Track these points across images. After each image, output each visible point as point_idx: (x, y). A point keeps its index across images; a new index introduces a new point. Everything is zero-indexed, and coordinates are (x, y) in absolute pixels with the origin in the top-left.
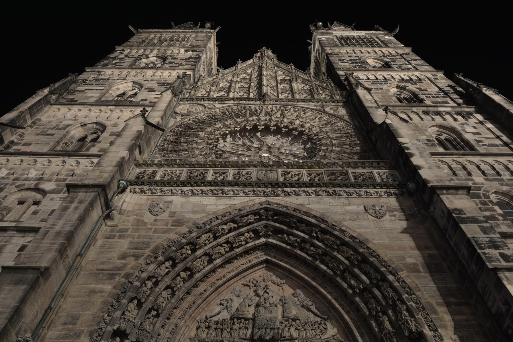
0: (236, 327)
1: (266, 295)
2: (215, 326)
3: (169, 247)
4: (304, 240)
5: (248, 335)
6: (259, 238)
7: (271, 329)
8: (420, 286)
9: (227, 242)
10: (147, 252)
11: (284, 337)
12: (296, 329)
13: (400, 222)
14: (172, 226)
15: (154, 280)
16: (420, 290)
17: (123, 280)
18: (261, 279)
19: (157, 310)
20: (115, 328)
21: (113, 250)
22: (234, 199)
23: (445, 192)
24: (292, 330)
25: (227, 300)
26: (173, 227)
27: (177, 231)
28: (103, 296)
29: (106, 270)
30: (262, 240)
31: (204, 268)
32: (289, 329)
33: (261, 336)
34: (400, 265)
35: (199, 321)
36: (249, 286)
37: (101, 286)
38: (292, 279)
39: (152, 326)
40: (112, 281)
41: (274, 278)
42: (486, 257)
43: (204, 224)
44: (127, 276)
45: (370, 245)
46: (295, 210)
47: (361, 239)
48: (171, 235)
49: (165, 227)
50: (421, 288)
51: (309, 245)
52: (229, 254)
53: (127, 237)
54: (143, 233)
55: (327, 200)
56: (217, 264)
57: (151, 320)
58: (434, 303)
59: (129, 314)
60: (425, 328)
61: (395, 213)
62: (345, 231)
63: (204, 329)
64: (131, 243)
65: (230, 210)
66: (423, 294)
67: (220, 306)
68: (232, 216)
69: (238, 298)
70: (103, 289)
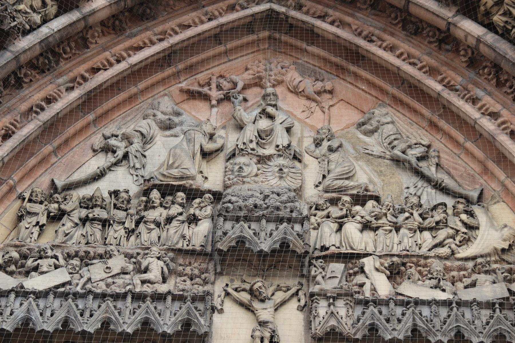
1: (264, 124)
2: (84, 213)
7: (280, 220)
11: (324, 248)
12: (366, 226)
18: (247, 76)
24: (352, 228)
25: (127, 139)
31: (45, 21)
32: (341, 226)
33: (241, 241)
35: (27, 195)
36: (206, 98)
38: (356, 75)
41: (293, 76)
56: (93, 13)
63: (43, 220)
69: (168, 133)
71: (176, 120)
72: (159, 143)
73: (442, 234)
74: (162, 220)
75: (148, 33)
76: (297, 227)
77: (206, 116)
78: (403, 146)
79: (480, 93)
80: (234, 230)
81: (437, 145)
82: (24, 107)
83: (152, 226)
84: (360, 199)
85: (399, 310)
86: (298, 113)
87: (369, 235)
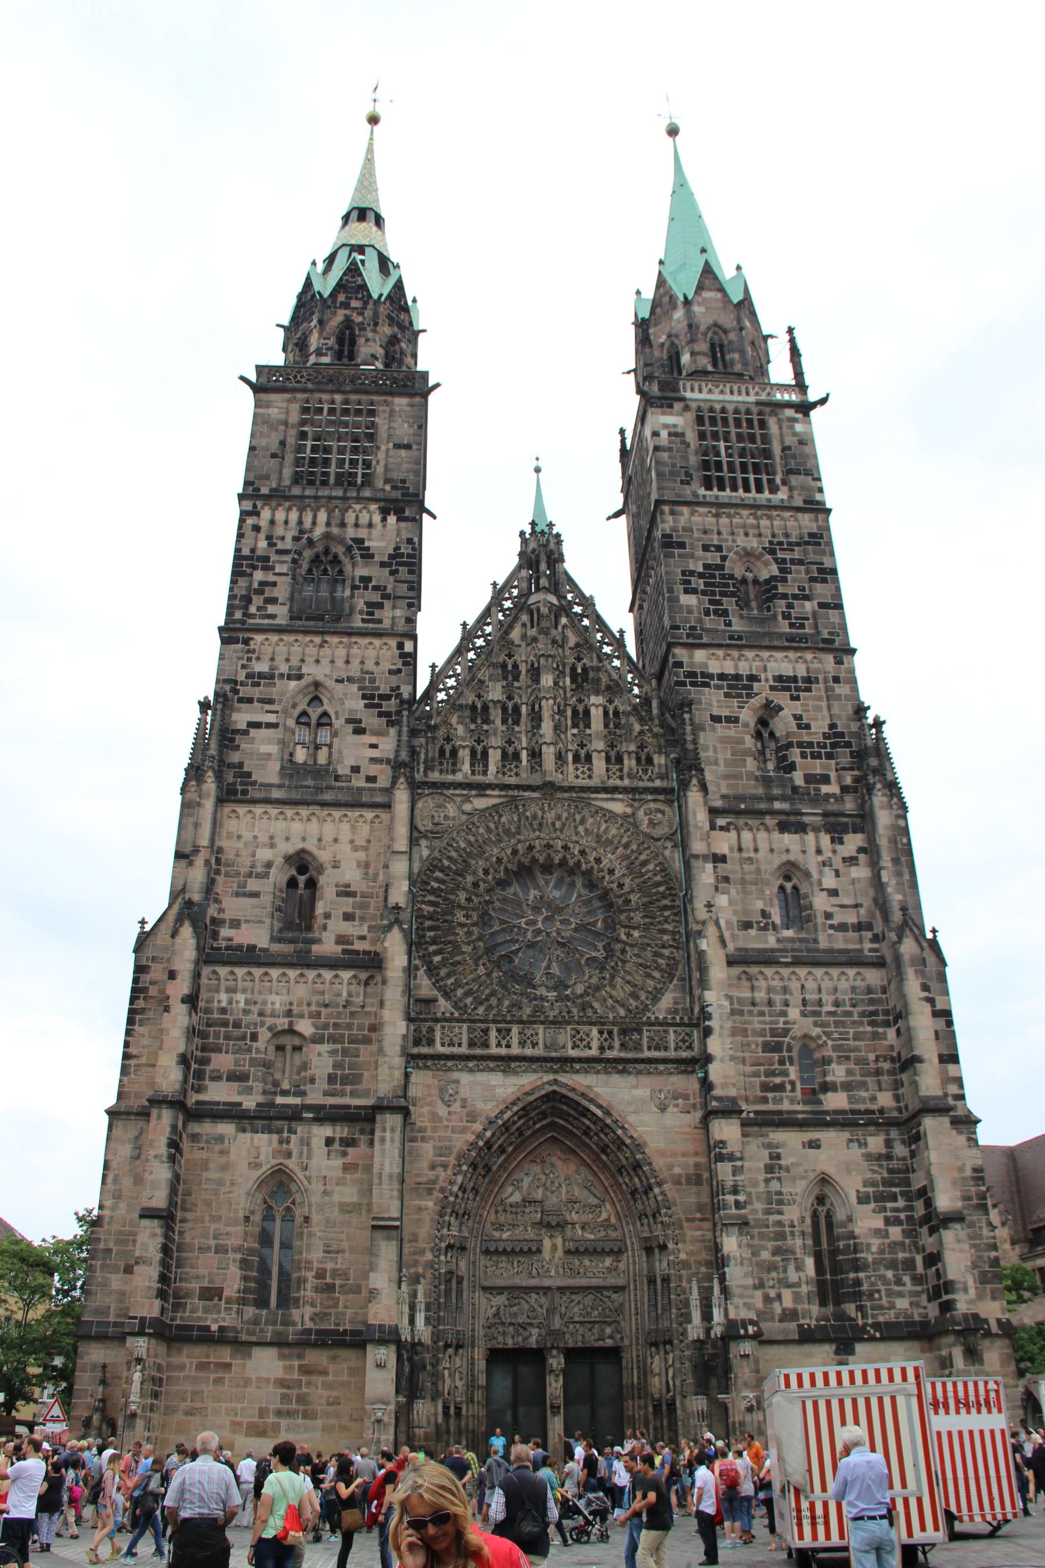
0: (527, 1210)
4: (588, 1128)
5: (538, 1220)
6: (545, 1117)
9: (518, 1129)
10: (452, 1160)
17: (441, 1196)
37: (423, 1203)
41: (559, 1153)
44: (442, 1190)
46: (583, 1095)
47: (640, 1141)
54: (442, 1134)
55: (616, 1078)
64: (435, 1147)
65: (519, 1095)
68: (521, 1105)
77: (536, 1168)
80: (546, 1219)
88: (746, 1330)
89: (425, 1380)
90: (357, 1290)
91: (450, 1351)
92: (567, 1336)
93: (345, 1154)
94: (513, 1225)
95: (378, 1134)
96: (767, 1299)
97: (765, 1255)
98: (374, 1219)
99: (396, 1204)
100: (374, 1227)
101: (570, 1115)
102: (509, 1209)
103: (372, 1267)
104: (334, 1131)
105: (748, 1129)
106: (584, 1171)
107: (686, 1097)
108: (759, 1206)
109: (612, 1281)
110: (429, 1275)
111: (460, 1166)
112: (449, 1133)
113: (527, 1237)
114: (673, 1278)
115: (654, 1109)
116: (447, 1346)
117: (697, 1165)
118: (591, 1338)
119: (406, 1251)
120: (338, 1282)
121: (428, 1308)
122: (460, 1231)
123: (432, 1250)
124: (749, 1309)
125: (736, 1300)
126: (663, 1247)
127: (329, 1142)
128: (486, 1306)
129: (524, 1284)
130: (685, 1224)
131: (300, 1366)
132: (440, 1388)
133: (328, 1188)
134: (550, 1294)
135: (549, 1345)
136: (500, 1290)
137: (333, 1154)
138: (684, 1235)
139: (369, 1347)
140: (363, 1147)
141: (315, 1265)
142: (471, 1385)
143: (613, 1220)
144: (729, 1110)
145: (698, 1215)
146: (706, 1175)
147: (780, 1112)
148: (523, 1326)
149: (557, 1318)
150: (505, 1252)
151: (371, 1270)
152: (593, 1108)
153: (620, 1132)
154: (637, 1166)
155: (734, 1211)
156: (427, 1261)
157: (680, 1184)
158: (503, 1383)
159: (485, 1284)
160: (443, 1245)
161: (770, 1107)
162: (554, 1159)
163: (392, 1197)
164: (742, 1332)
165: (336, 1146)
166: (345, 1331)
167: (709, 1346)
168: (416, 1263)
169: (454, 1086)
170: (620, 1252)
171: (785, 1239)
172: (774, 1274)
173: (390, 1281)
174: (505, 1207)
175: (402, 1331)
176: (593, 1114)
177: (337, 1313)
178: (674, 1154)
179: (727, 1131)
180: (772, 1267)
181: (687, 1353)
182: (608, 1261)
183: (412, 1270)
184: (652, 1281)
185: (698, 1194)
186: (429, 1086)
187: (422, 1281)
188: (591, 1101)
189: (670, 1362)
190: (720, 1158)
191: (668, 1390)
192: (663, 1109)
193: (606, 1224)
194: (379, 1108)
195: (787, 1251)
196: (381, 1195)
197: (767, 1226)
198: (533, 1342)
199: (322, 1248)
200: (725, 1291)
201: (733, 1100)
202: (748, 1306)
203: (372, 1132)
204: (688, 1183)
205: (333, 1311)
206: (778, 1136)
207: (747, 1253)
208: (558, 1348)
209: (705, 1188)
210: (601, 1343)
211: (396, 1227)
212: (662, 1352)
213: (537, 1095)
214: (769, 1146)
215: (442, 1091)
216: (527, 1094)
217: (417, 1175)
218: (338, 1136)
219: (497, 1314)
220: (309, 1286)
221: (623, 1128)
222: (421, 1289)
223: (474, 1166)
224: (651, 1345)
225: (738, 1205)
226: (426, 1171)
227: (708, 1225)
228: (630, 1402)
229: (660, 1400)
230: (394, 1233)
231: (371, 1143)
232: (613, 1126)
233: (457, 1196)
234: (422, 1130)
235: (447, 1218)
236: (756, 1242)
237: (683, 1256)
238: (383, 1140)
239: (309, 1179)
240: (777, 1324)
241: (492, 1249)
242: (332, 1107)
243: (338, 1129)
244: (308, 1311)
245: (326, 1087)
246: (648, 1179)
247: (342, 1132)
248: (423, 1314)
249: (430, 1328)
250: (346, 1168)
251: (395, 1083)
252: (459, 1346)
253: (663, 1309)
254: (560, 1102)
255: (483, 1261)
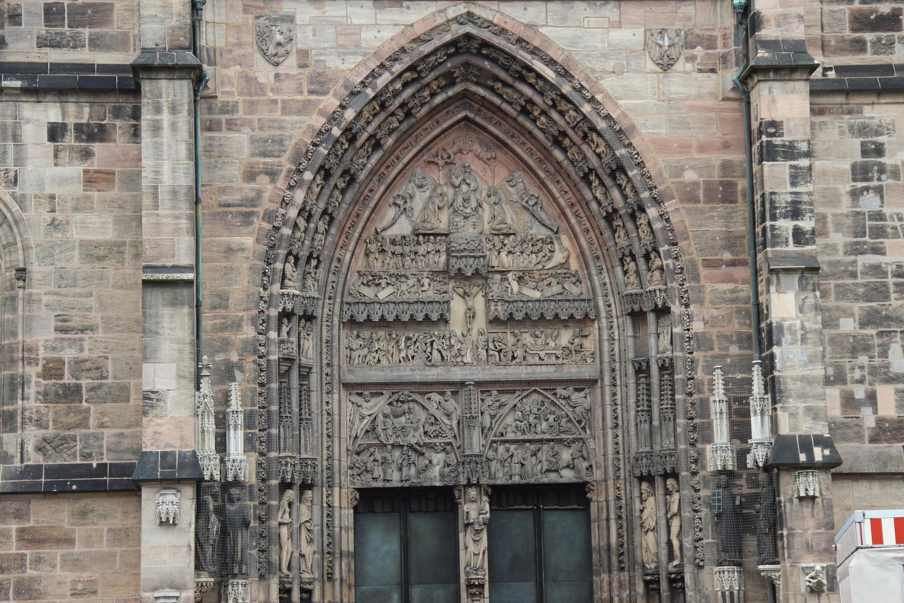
0: (422, 249)
1: (464, 188)
3: (314, 145)
4: (530, 101)
5: (441, 266)
6: (452, 83)
8: (689, 229)
9: (403, 105)
10: (285, 163)
11: (493, 267)
12: (510, 252)
13: (701, 76)
14: (311, 92)
15: (307, 214)
16: (686, 238)
17: (267, 226)
18: (455, 149)
19: (318, 258)
20: (280, 310)
21: (230, 159)
22: (408, 8)
23: (771, 74)
24: (503, 254)
25: (403, 198)
26: (313, 97)
27: (321, 106)
28: (248, 258)
29: (233, 205)
30: (458, 89)
31: (368, 158)
33: (460, 270)
34: (672, 187)
39: (316, 284)
40: (250, 228)
41: (477, 147)
42: (773, 235)
43: (362, 82)
44: (269, 216)
45: (635, 142)
46: (520, 41)
47: (623, 124)
48: (314, 116)
49: (299, 97)
50: (690, 234)
51: (539, 111)
52: (405, 126)
53: (242, 125)
54: (266, 116)
57: (313, 275)
58: (700, 262)
59: (291, 284)
60: (673, 303)
61: (699, 51)
62: (600, 104)
64: (252, 140)
65: (403, 42)
66: (689, 244)
67: (393, 207)
68: (407, 61)
70: (243, 244)
71: (424, 183)
72: (417, 197)
73: (541, 255)
74: (425, 253)
75: (410, 139)
76: (482, 259)
77: (438, 176)
78: (526, 199)
79: (561, 180)
80: (456, 264)
81: (542, 197)
82: (362, 199)
83: (422, 258)
84: (507, 235)
85: (521, 304)
86: (479, 172)
87: (511, 256)
88: (810, 454)
89: (246, 544)
90: (121, 394)
91: (291, 494)
92: (494, 465)
93: (87, 155)
94: (398, 276)
95: (147, 116)
96: (849, 401)
97: (848, 326)
98: (146, 268)
99: (186, 242)
100: (146, 283)
101: (496, 78)
102: (389, 248)
103: (147, 355)
104: (64, 114)
105: (823, 100)
106: (521, 176)
107: (710, 43)
108: (839, 239)
109: (572, 370)
110: (249, 365)
111: (300, 172)
112: (278, 115)
113: (423, 297)
114: (679, 365)
115: (650, 65)
116: (285, 486)
117: (726, 166)
118: (535, 469)
119: (207, 323)
120: (84, 382)
121: (249, 421)
122: (304, 287)
123: (253, 321)
124: (816, 417)
125: (791, 403)
126: (663, 312)
127: (55, 132)
128: (352, 416)
129: (418, 378)
130: (703, 272)
131: (21, 531)
132: (274, 558)
133: (59, 216)
134: (463, 394)
135: (463, 481)
136: (377, 388)
137: (64, 156)
138: (701, 290)
139: (146, 493)
140: (120, 142)
141: (42, 353)
142: (328, 552)
143: (574, 265)
144: (791, 66)
145: (727, 256)
146: (742, 184)
147: (888, 68)
148: (417, 450)
149: (476, 434)
150: (383, 322)
151: (145, 359)
152: (539, 66)
153: (586, 108)
154: (618, 170)
155: (791, 247)
156: (245, 342)
157: (696, 200)
158: (384, 546)
159: (350, 378)
160: (274, 312)
161: (869, 58)
162: (469, 159)
163: (177, 231)
164: (803, 457)
165: (70, 139)
166: (102, 466)
167: (743, 482)
168: (226, 345)
169: (284, 27)
170: (586, 320)
171: (887, 298)
172: (863, 359)
173: (180, 376)
174: (382, 245)
175: (204, 463)
176: (539, 76)
177: (87, 437)
178: (684, 148)
179: (784, 104)
180: (859, 347)
181: (704, 493)
182: (566, 337)
183: (219, 358)
184: (642, 370)
185: (728, 218)
186: (237, 28)
187: (238, 374)
188: (535, 52)
189: (674, 508)
190: (770, 153)
191: (671, 557)
192: (666, 65)
193: (563, 273)
194: (144, 70)
195: (888, 318)
196: (158, 227)
197: (854, 275)
198: (435, 477)
199: (53, 323)
200: (772, 386)
201: (798, 47)
202: (814, 414)
203: (136, 114)
204: (710, 199)
205: (78, 432)
206: (879, 112)
207: (814, 322)
208: (478, 485)
209: (741, 209)
210: (552, 478)
211: (189, 283)
212: (660, 491)
213: (437, 43)
214: (863, 130)
215: (262, 37)
216: (418, 40)
217: (223, 191)
218: (71, 121)
219: (371, 430)
220: (31, 391)
221: (592, 100)
222: (235, 391)
223: (325, 172)
224: (641, 479)
225: (798, 235)
226: (239, 183)
227: (744, 272)
228: (605, 576)
229: (657, 573)
230: (185, 292)
231: (136, 134)
232: (575, 97)
233: (296, 226)
234: (229, 108)
235: (279, 265)
236: (832, 302)
237: (697, 327)
238: (156, 128)
239: (21, 201)
240: (867, 446)
241: (361, 318)
242: (56, 67)
243: (71, 108)
244: (32, 435)
245: (43, 30)
246: (636, 193)
247: (79, 114)
248: (240, 433)
249: (254, 456)
250: (91, 180)
251: (174, 22)
252: (306, 486)
253: (663, 419)
254: (479, 54)
255: (346, 338)
